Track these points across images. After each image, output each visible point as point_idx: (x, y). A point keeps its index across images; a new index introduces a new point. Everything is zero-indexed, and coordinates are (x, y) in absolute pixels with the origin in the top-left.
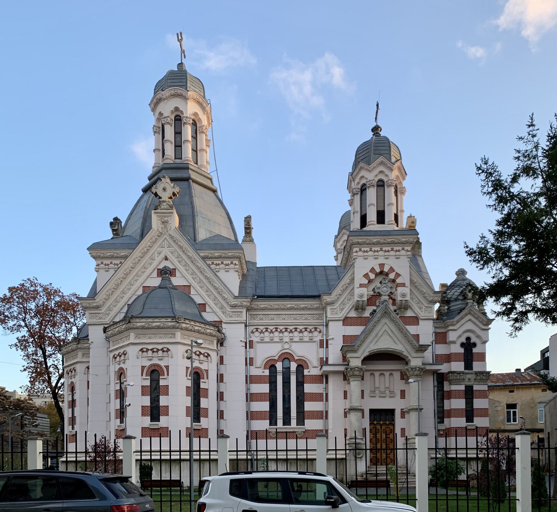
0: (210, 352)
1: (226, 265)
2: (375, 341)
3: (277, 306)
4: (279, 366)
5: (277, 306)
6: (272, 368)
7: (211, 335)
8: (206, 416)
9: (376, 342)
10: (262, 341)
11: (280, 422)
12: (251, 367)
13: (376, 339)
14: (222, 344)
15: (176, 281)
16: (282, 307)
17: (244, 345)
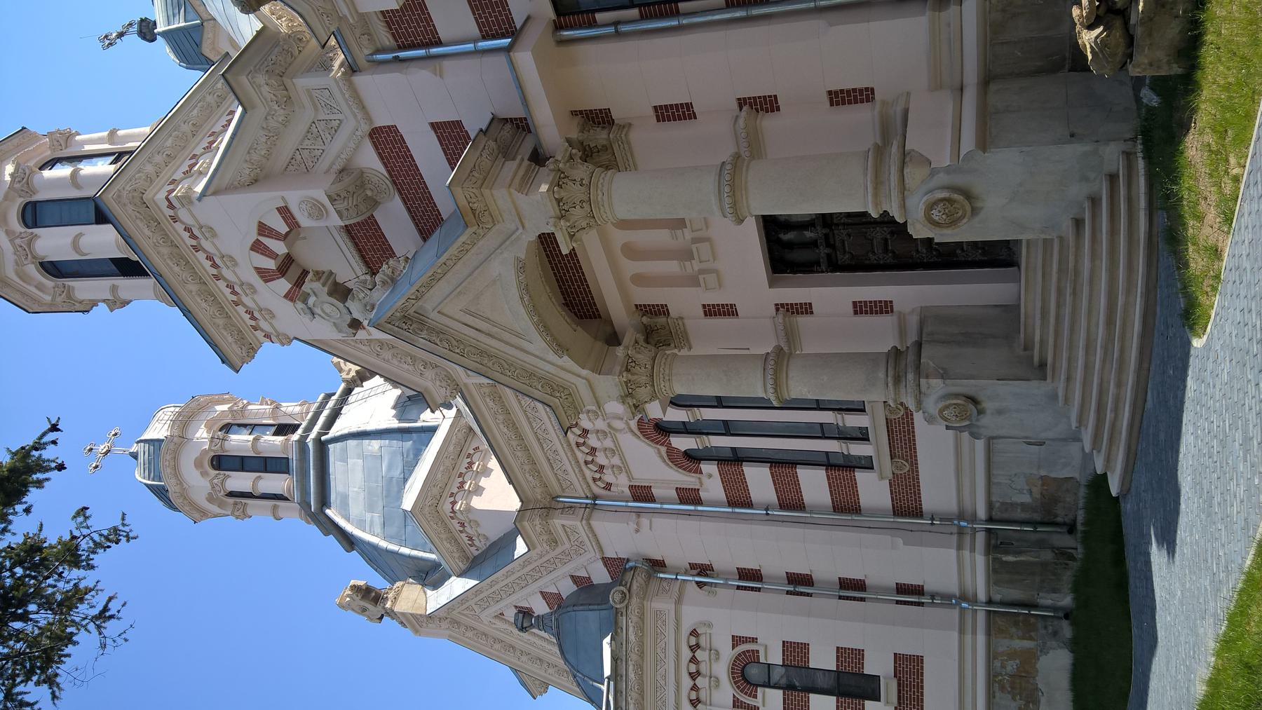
0: (685, 631)
1: (463, 525)
2: (515, 340)
3: (519, 454)
4: (682, 443)
5: (519, 454)
6: (692, 459)
7: (641, 628)
8: (859, 655)
9: (518, 335)
10: (624, 468)
11: (858, 449)
12: (703, 495)
13: (506, 336)
14: (657, 565)
15: (541, 608)
16: (514, 443)
17: (645, 521)
